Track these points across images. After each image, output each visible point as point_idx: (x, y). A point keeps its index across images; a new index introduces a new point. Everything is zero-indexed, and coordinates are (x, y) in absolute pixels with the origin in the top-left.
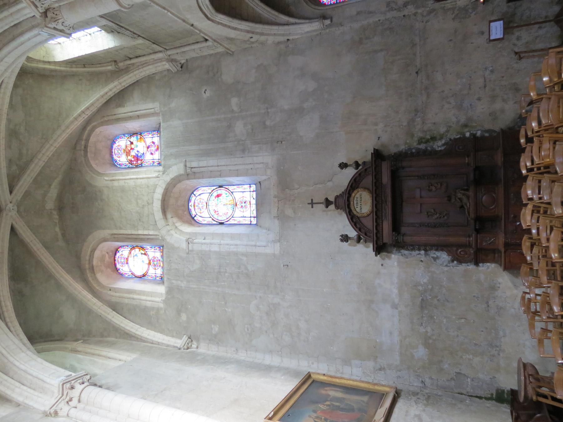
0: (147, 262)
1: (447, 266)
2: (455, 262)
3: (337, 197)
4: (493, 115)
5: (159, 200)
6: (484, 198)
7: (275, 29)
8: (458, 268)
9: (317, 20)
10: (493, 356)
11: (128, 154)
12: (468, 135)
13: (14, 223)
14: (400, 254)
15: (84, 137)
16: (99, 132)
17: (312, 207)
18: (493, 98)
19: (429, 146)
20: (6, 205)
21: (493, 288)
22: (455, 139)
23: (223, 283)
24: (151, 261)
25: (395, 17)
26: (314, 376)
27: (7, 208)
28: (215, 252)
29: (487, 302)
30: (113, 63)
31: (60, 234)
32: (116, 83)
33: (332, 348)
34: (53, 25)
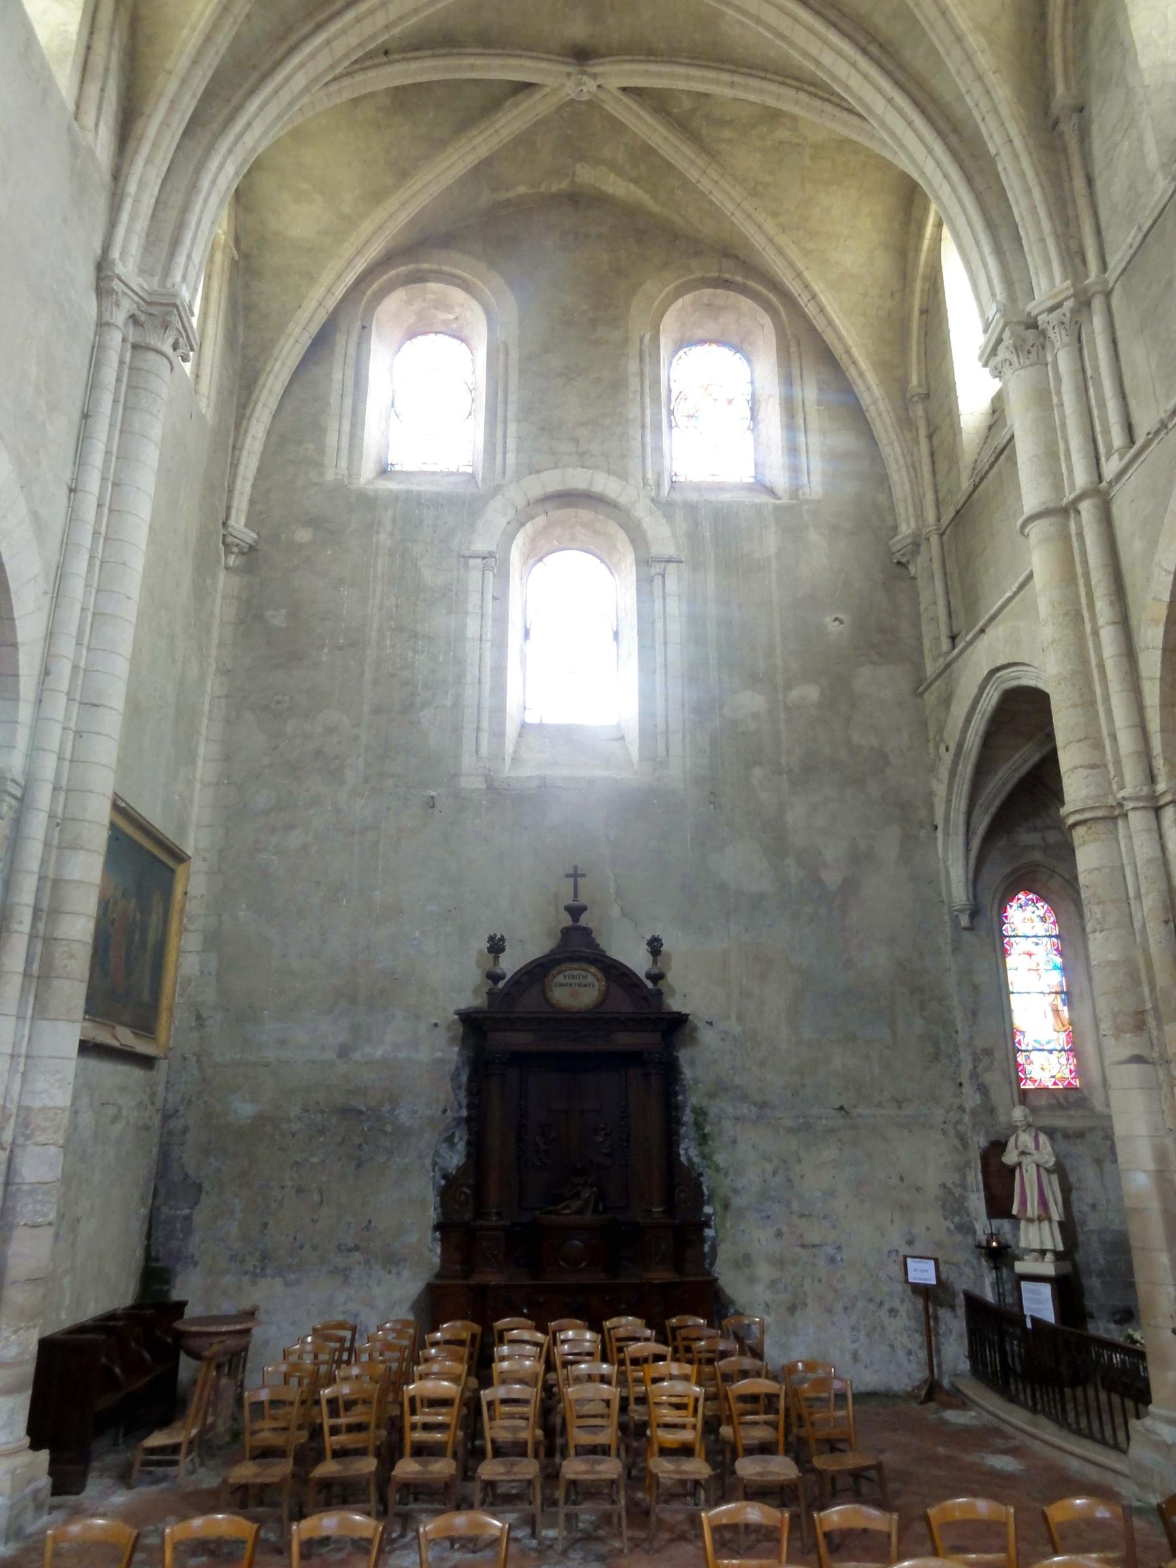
1: (435, 1164)
2: (443, 1182)
3: (587, 932)
4: (744, 1262)
5: (591, 483)
6: (577, 1242)
8: (431, 1187)
9: (971, 897)
10: (243, 1262)
12: (708, 1209)
13: (546, 91)
14: (460, 1065)
15: (752, 284)
16: (762, 321)
17: (568, 876)
19: (687, 1130)
20: (594, 76)
21: (391, 1261)
22: (701, 1184)
23: (388, 643)
25: (959, 1066)
26: (180, 870)
27: (585, 78)
28: (464, 626)
29: (356, 1248)
30: (923, 390)
31: (511, 194)
32: (877, 392)
33: (244, 906)
34: (1008, 341)
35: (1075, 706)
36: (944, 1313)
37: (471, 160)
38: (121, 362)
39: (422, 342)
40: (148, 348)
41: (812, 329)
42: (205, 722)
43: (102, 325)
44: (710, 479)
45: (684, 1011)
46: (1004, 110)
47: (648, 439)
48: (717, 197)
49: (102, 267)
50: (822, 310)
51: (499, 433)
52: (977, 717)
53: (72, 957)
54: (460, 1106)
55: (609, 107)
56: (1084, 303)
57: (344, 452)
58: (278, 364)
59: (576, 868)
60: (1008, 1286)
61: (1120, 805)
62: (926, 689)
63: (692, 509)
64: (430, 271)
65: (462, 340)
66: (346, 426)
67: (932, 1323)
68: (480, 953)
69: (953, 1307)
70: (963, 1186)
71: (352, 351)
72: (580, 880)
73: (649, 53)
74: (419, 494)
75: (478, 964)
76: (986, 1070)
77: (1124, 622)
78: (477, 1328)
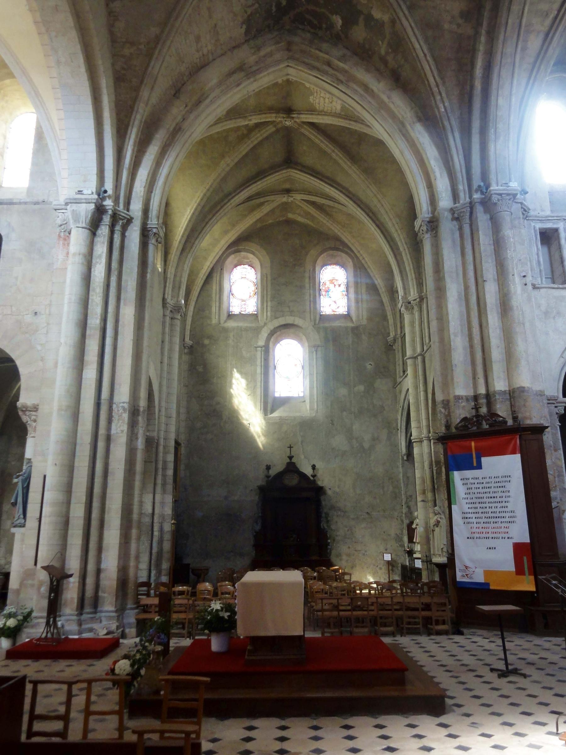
0: (244, 298)
2: (255, 534)
3: (294, 464)
11: (332, 281)
12: (329, 541)
15: (345, 249)
20: (292, 197)
24: (244, 302)
35: (415, 411)
37: (254, 220)
39: (239, 267)
40: (175, 318)
41: (363, 265)
43: (164, 316)
44: (333, 313)
45: (323, 485)
49: (164, 300)
57: (217, 313)
59: (290, 445)
64: (242, 249)
65: (252, 267)
70: (402, 534)
72: (292, 449)
73: (310, 193)
76: (410, 501)
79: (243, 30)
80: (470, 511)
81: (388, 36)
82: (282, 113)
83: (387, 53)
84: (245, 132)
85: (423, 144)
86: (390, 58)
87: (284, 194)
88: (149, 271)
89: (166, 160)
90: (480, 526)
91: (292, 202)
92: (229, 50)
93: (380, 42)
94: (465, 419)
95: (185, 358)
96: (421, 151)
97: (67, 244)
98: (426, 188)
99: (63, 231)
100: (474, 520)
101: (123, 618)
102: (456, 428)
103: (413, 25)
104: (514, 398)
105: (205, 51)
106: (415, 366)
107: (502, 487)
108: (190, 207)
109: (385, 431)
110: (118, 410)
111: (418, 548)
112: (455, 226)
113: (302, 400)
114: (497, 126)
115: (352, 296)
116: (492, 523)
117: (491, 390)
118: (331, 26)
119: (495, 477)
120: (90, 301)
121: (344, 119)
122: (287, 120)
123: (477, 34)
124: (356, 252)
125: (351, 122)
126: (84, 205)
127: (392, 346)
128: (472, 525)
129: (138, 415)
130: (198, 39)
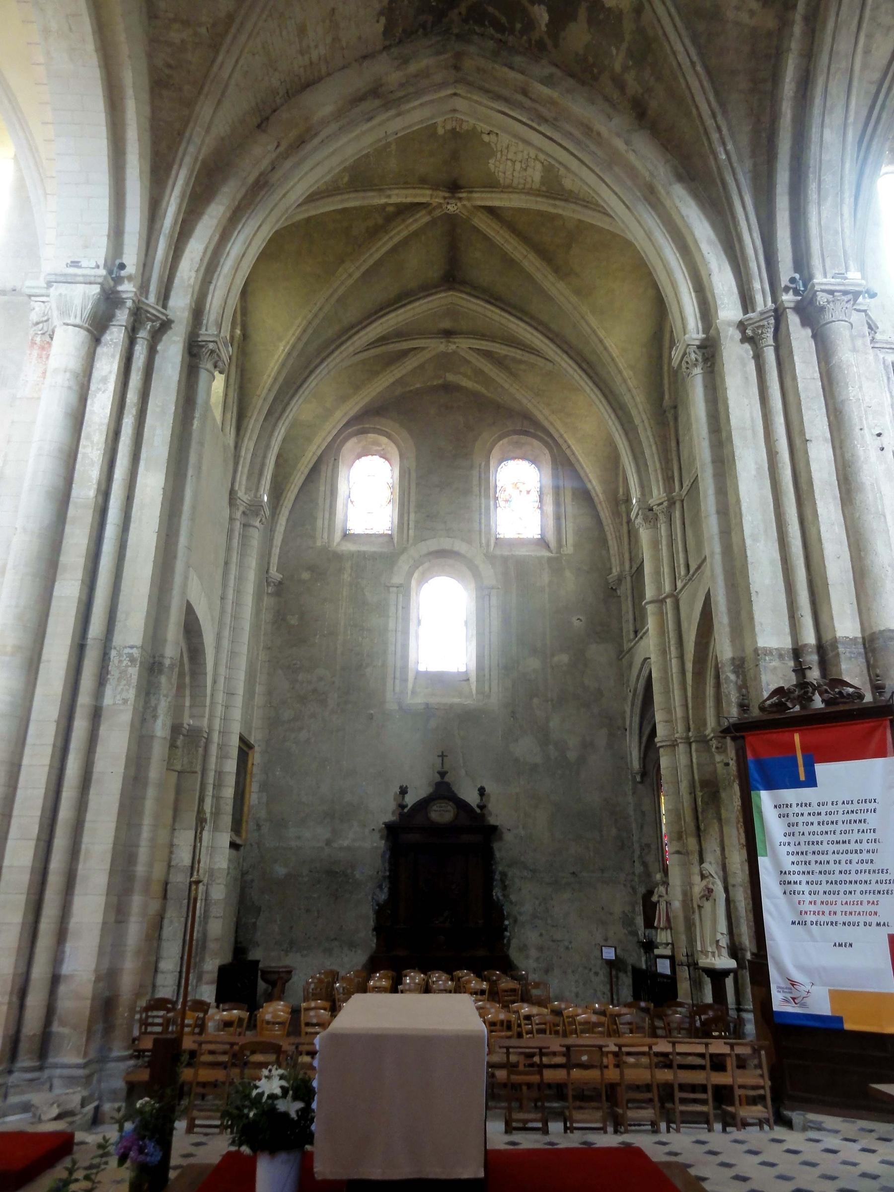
1: (373, 898)
3: (448, 785)
4: (523, 948)
7: (636, 719)
15: (540, 434)
17: (439, 756)
18: (541, 949)
20: (455, 343)
21: (352, 945)
26: (250, 753)
29: (336, 939)
31: (412, 388)
36: (621, 975)
37: (391, 380)
38: (239, 534)
39: (364, 459)
40: (250, 526)
41: (568, 460)
42: (259, 675)
43: (232, 519)
44: (516, 536)
46: (641, 408)
47: (483, 521)
48: (518, 396)
49: (232, 492)
50: (574, 454)
51: (406, 518)
52: (641, 677)
53: (227, 805)
54: (385, 870)
55: (462, 353)
56: (672, 503)
57: (326, 530)
58: (293, 486)
60: (653, 961)
61: (676, 740)
62: (623, 657)
63: (505, 559)
65: (386, 459)
66: (327, 516)
67: (614, 980)
68: (396, 793)
69: (626, 972)
70: (633, 911)
71: (329, 474)
72: (445, 758)
73: (483, 336)
74: (364, 552)
75: (395, 799)
77: (681, 657)
78: (394, 974)
79: (380, 27)
80: (795, 868)
81: (628, 37)
82: (443, 191)
83: (625, 68)
84: (380, 221)
85: (688, 216)
86: (630, 78)
87: (442, 338)
88: (197, 415)
89: (239, 232)
90: (819, 898)
91: (454, 352)
92: (356, 61)
93: (614, 51)
94: (779, 691)
95: (267, 601)
96: (684, 230)
97: (44, 356)
98: (692, 290)
99: (40, 332)
100: (804, 887)
101: (99, 1081)
102: (762, 709)
103: (673, 10)
104: (874, 651)
105: (315, 55)
106: (661, 614)
107: (860, 821)
108: (284, 343)
109: (604, 731)
110: (120, 661)
111: (663, 937)
112: (747, 351)
113: (465, 678)
114: (822, 178)
115: (549, 508)
116: (841, 893)
117: (827, 637)
118: (530, 25)
119: (843, 803)
120: (80, 456)
121: (547, 197)
122: (450, 201)
123: (784, 24)
124: (556, 436)
125: (557, 203)
126: (80, 289)
127: (615, 590)
128: (801, 897)
129: (160, 672)
130: (302, 30)
